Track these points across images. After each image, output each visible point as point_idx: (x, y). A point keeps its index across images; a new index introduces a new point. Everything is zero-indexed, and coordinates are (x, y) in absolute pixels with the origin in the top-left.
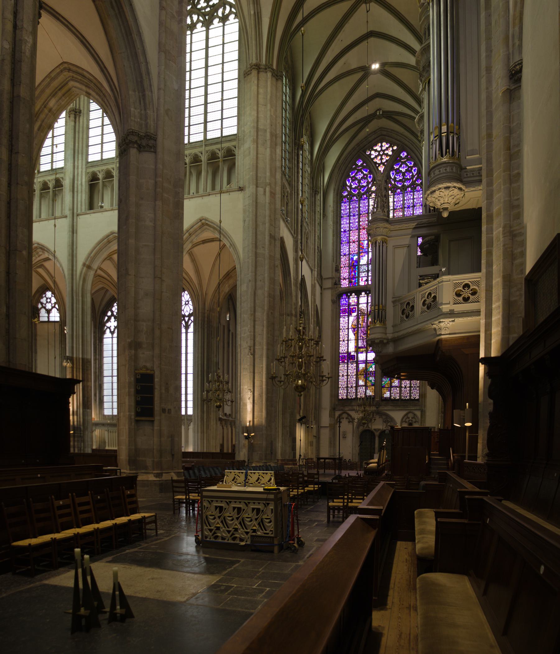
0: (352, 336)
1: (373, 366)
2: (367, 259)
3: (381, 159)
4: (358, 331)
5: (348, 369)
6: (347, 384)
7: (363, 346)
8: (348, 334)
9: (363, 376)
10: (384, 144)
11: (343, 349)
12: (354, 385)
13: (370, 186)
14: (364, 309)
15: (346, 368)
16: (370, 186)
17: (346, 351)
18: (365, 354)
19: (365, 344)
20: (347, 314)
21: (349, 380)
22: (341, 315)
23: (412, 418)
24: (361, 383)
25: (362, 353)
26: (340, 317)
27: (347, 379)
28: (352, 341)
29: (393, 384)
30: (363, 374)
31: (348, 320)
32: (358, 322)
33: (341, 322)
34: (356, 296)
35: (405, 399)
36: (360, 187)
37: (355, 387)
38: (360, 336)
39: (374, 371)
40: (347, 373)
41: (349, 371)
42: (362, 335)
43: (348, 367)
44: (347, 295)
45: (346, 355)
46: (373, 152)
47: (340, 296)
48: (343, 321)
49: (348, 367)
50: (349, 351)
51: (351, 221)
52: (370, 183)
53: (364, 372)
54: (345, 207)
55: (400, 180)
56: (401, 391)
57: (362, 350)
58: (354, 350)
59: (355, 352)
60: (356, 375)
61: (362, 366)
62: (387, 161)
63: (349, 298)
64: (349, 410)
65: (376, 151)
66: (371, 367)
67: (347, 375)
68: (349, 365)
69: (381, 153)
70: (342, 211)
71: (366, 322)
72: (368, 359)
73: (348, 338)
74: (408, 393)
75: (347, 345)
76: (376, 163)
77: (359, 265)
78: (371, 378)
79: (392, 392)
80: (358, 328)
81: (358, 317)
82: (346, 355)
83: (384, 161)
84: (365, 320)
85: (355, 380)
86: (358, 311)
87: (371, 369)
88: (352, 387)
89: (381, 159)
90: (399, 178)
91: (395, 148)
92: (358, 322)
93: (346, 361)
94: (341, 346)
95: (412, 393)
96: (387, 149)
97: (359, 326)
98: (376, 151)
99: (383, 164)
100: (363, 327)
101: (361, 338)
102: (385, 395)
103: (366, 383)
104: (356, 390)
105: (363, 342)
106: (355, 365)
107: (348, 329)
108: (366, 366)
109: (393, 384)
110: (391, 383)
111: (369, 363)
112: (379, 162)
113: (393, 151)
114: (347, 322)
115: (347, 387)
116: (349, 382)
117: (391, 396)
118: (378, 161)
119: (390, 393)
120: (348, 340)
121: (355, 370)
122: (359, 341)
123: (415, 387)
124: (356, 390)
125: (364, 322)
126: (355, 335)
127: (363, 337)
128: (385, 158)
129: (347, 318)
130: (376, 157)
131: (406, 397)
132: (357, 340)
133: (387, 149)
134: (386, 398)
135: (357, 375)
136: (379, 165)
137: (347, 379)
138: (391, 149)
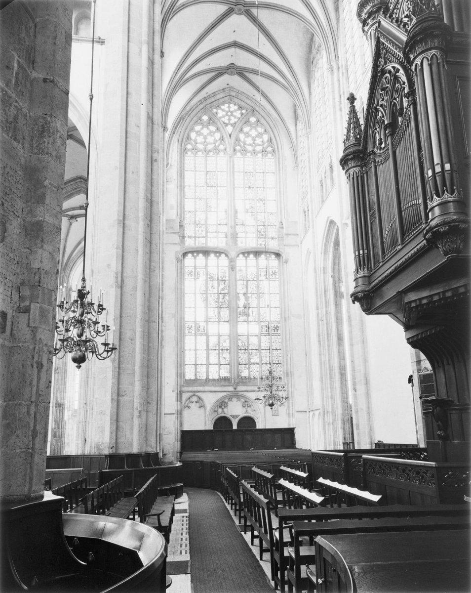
0: (201, 303)
1: (228, 341)
3: (229, 120)
4: (207, 297)
10: (232, 105)
11: (189, 317)
13: (217, 144)
16: (217, 144)
21: (197, 356)
24: (213, 359)
27: (196, 354)
32: (207, 288)
36: (205, 143)
42: (212, 302)
44: (193, 256)
46: (219, 111)
47: (185, 254)
48: (189, 285)
51: (197, 177)
52: (217, 141)
54: (189, 159)
55: (250, 145)
61: (213, 341)
66: (225, 342)
69: (229, 114)
70: (186, 165)
71: (216, 287)
77: (206, 224)
79: (251, 370)
80: (207, 293)
83: (232, 122)
86: (207, 274)
87: (225, 344)
89: (229, 120)
90: (249, 141)
91: (244, 111)
92: (207, 288)
96: (235, 111)
97: (209, 292)
98: (223, 110)
99: (232, 125)
103: (219, 360)
107: (195, 294)
108: (219, 340)
109: (252, 361)
110: (249, 359)
112: (227, 121)
117: (250, 375)
120: (195, 308)
128: (233, 120)
130: (224, 117)
135: (208, 349)
136: (226, 125)
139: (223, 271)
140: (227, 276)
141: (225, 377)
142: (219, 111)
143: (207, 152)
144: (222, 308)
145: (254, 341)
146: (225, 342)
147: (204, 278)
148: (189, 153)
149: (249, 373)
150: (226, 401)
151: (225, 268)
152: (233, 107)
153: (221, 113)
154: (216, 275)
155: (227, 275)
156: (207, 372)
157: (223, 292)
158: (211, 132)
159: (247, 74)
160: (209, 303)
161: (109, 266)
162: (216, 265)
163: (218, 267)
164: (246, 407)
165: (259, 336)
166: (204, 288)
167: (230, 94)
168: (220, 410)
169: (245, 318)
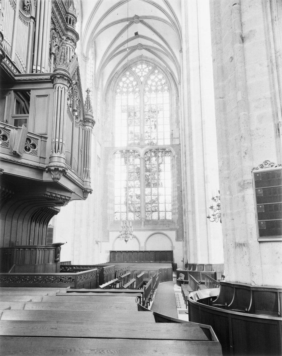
3: (142, 74)
62: (145, 75)
65: (138, 68)
69: (142, 70)
76: (138, 76)
83: (143, 75)
89: (142, 74)
91: (150, 68)
96: (145, 68)
98: (138, 68)
99: (143, 77)
112: (140, 75)
113: (149, 70)
118: (140, 74)
128: (144, 74)
133: (145, 68)
136: (141, 77)
138: (147, 69)
142: (137, 69)
143: (128, 92)
148: (118, 94)
152: (144, 66)
153: (137, 70)
158: (130, 81)
161: (119, 207)
167: (141, 59)
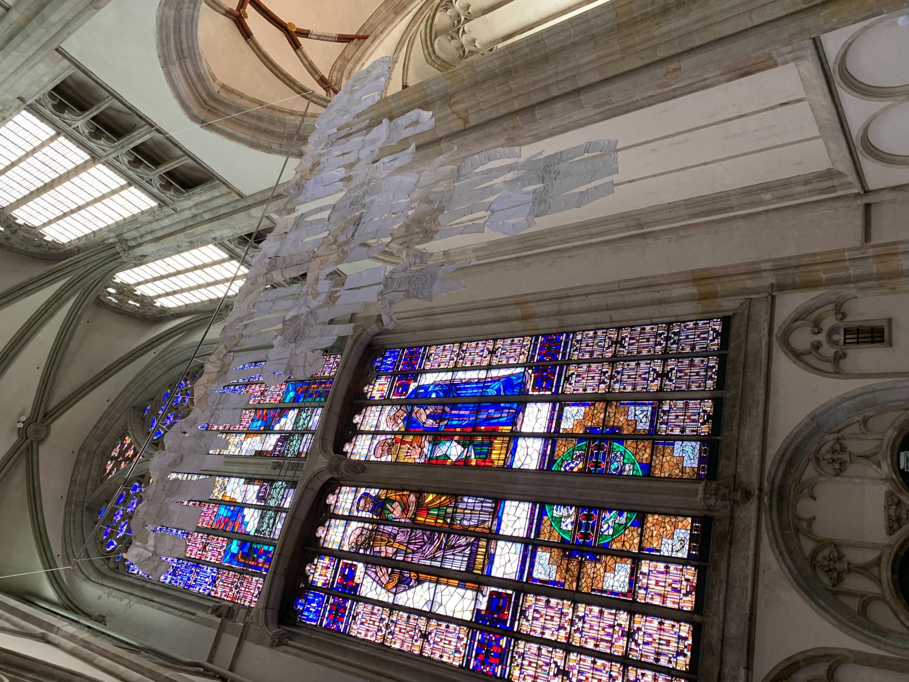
1: (558, 512)
2: (252, 510)
5: (542, 641)
6: (610, 658)
7: (467, 552)
8: (411, 611)
9: (589, 567)
12: (623, 617)
14: (358, 532)
15: (534, 647)
17: (463, 632)
18: (501, 543)
19: (463, 541)
20: (348, 605)
21: (590, 645)
22: (342, 627)
23: (817, 327)
25: (490, 558)
26: (347, 635)
27: (582, 650)
28: (438, 598)
29: (640, 426)
30: (581, 565)
31: (367, 601)
33: (362, 636)
34: (315, 562)
35: (718, 373)
37: (632, 614)
38: (433, 558)
39: (577, 512)
40: (555, 644)
41: (547, 635)
42: (429, 550)
43: (529, 639)
45: (479, 636)
49: (529, 639)
50: (468, 616)
53: (570, 557)
56: (676, 394)
57: (480, 558)
58: (470, 594)
59: (479, 591)
60: (575, 603)
63: (312, 586)
64: (749, 668)
66: (559, 520)
67: (568, 648)
68: (525, 627)
71: (395, 530)
72: (522, 533)
73: (420, 613)
74: (692, 364)
75: (444, 625)
78: (607, 529)
79: (677, 431)
81: (373, 561)
82: (479, 636)
84: (389, 534)
85: (596, 609)
88: (630, 635)
93: (503, 642)
94: (437, 657)
95: (693, 348)
100: (409, 543)
101: (439, 554)
102: (687, 464)
103: (622, 554)
104: (648, 610)
105: (453, 547)
106: (531, 598)
107: (393, 607)
108: (548, 545)
110: (636, 437)
111: (538, 533)
114: (370, 607)
115: (625, 661)
116: (603, 647)
119: (683, 438)
120: (430, 616)
121: (553, 602)
122: (448, 566)
123: (667, 339)
124: (648, 610)
125: (395, 536)
126: (420, 582)
127: (439, 548)
129: (361, 606)
131: (708, 368)
132: (440, 576)
134: (701, 460)
135: (576, 597)
137: (582, 650)
139: (362, 502)
140: (377, 491)
141: (693, 538)
144: (453, 519)
145: (572, 418)
146: (559, 520)
147: (361, 567)
149: (689, 439)
150: (808, 546)
151: (359, 496)
154: (367, 525)
155: (373, 492)
156: (662, 613)
157: (412, 508)
159: (54, 402)
160: (428, 563)
162: (343, 522)
163: (349, 519)
164: (845, 457)
165: (559, 402)
166: (383, 573)
168: (857, 583)
169: (497, 443)
